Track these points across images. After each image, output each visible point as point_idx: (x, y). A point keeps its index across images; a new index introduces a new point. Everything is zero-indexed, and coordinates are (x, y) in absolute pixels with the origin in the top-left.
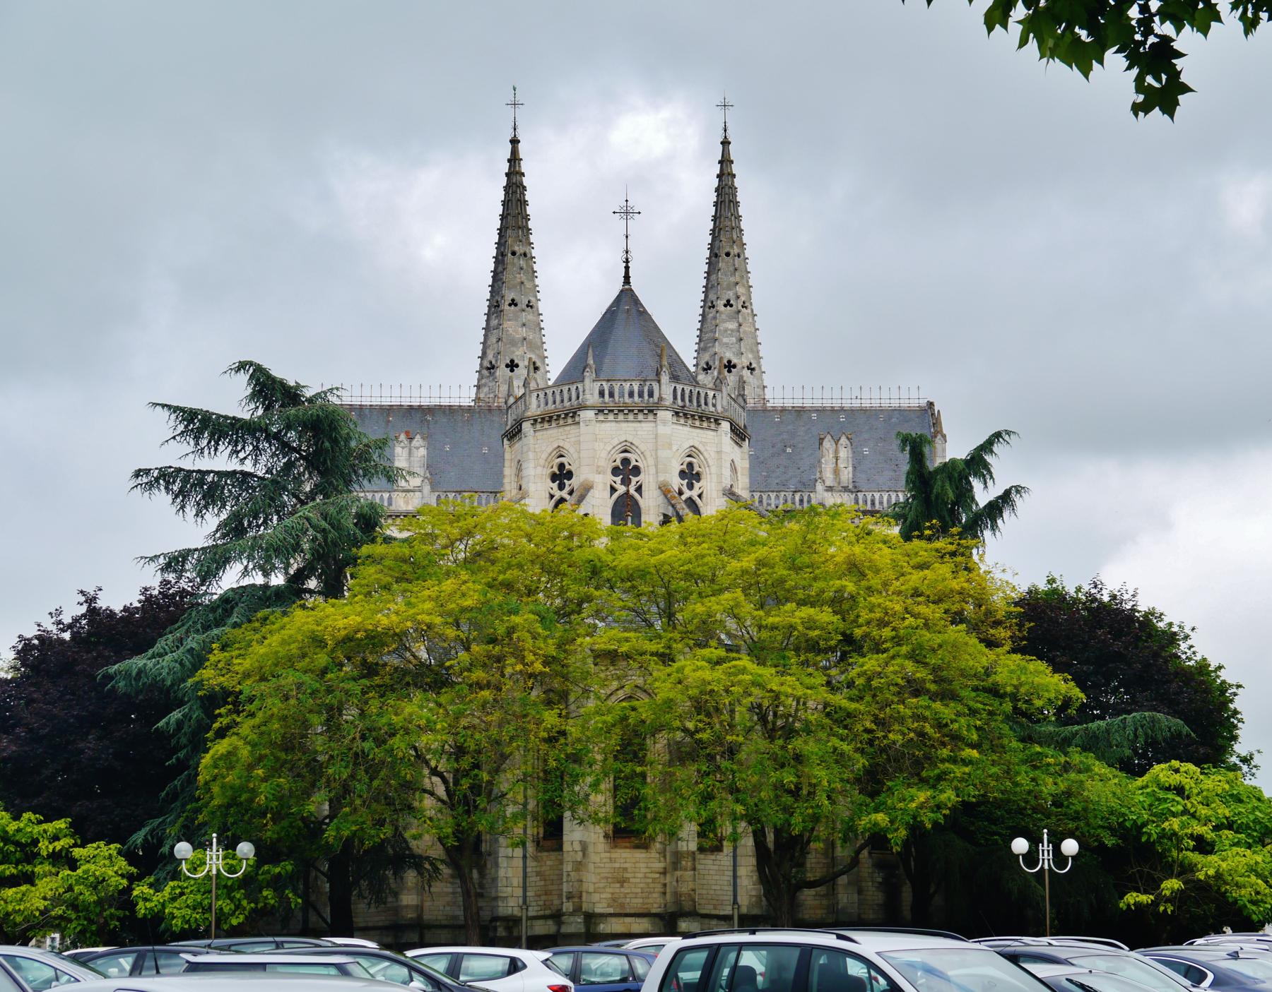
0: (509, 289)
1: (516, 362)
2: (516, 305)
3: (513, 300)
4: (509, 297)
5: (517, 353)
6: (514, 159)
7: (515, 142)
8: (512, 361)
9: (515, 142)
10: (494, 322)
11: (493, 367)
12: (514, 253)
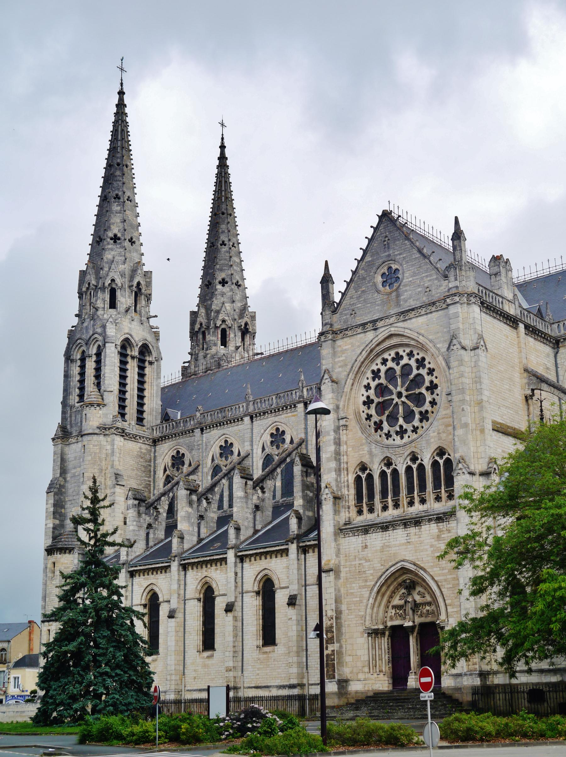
0: (127, 189)
1: (134, 240)
2: (131, 201)
3: (129, 197)
4: (128, 194)
5: (135, 234)
6: (121, 105)
7: (121, 93)
8: (132, 238)
9: (121, 93)
10: (116, 207)
11: (119, 239)
12: (127, 166)
